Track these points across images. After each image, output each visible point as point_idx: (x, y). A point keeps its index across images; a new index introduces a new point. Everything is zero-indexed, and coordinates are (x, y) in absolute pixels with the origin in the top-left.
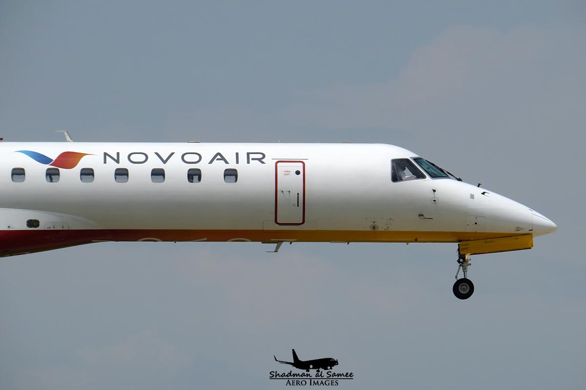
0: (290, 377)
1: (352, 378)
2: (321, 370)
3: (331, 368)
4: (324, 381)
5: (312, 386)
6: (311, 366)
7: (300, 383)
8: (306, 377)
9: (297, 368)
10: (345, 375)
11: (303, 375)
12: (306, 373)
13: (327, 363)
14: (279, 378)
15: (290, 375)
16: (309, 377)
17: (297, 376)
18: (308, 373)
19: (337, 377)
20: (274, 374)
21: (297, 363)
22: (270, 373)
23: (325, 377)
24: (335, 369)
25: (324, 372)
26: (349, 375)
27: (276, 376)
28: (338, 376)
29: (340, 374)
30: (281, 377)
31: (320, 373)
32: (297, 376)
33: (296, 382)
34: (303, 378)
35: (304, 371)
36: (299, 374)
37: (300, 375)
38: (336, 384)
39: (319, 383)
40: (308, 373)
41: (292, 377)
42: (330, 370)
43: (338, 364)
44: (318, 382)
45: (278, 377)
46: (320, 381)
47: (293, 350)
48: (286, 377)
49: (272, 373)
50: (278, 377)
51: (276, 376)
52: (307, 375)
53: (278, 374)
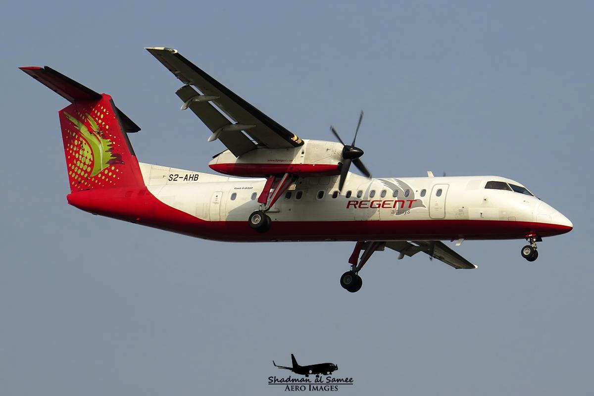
0: (289, 382)
1: (352, 383)
2: (320, 375)
3: (331, 374)
4: (323, 386)
5: (311, 391)
6: (311, 372)
7: (299, 389)
8: (305, 383)
9: (296, 373)
10: (344, 380)
11: (302, 380)
12: (305, 378)
13: (327, 368)
14: (278, 383)
15: (289, 380)
16: (308, 382)
17: (296, 381)
18: (308, 378)
19: (336, 382)
20: (273, 379)
21: (296, 368)
22: (269, 378)
23: (324, 382)
24: (335, 375)
25: (324, 378)
26: (348, 380)
27: (275, 381)
28: (338, 382)
29: (340, 379)
30: (280, 383)
31: (319, 379)
32: (296, 381)
33: (295, 387)
34: (302, 383)
35: (304, 376)
36: (298, 380)
37: (299, 380)
38: (336, 390)
39: (319, 389)
40: (308, 378)
41: (291, 382)
42: (330, 375)
43: (337, 369)
44: (317, 387)
45: (277, 382)
46: (319, 387)
47: (292, 355)
48: (285, 383)
49: (271, 378)
50: (277, 382)
51: (275, 381)
52: (307, 380)
53: (277, 380)
